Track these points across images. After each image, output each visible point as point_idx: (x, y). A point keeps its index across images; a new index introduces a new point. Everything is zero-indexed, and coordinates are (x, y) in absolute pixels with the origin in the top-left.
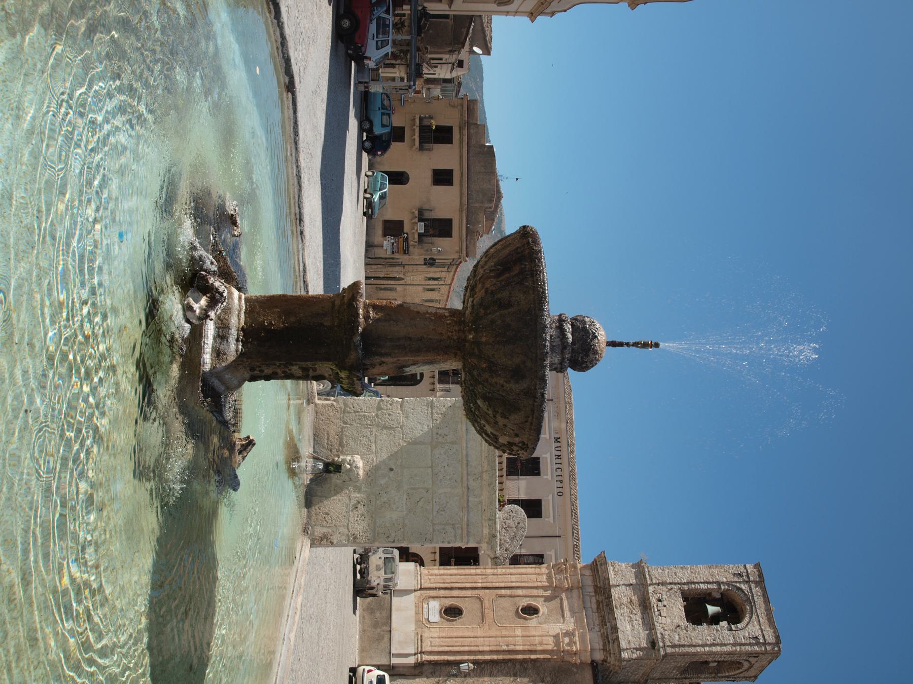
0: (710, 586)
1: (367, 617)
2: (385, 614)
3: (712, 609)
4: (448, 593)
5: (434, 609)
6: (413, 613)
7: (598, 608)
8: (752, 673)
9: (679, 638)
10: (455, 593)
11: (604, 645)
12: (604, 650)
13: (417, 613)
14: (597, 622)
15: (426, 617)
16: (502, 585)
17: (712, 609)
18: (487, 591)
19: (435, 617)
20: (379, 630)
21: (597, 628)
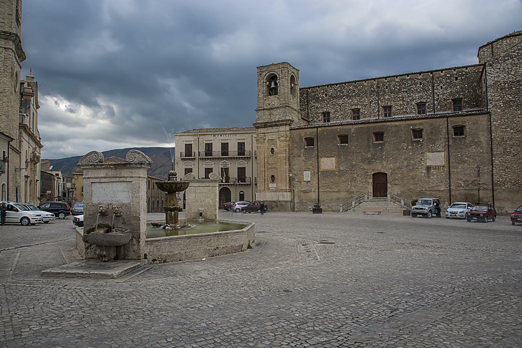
0: (264, 86)
1: (274, 209)
2: (273, 203)
3: (273, 86)
4: (266, 181)
5: (273, 186)
6: (273, 193)
7: (272, 127)
8: (295, 71)
9: (282, 98)
10: (266, 178)
11: (284, 125)
12: (286, 125)
13: (273, 192)
14: (276, 127)
15: (274, 188)
16: (264, 161)
17: (273, 86)
18: (266, 166)
19: (275, 185)
20: (279, 205)
21: (278, 127)
